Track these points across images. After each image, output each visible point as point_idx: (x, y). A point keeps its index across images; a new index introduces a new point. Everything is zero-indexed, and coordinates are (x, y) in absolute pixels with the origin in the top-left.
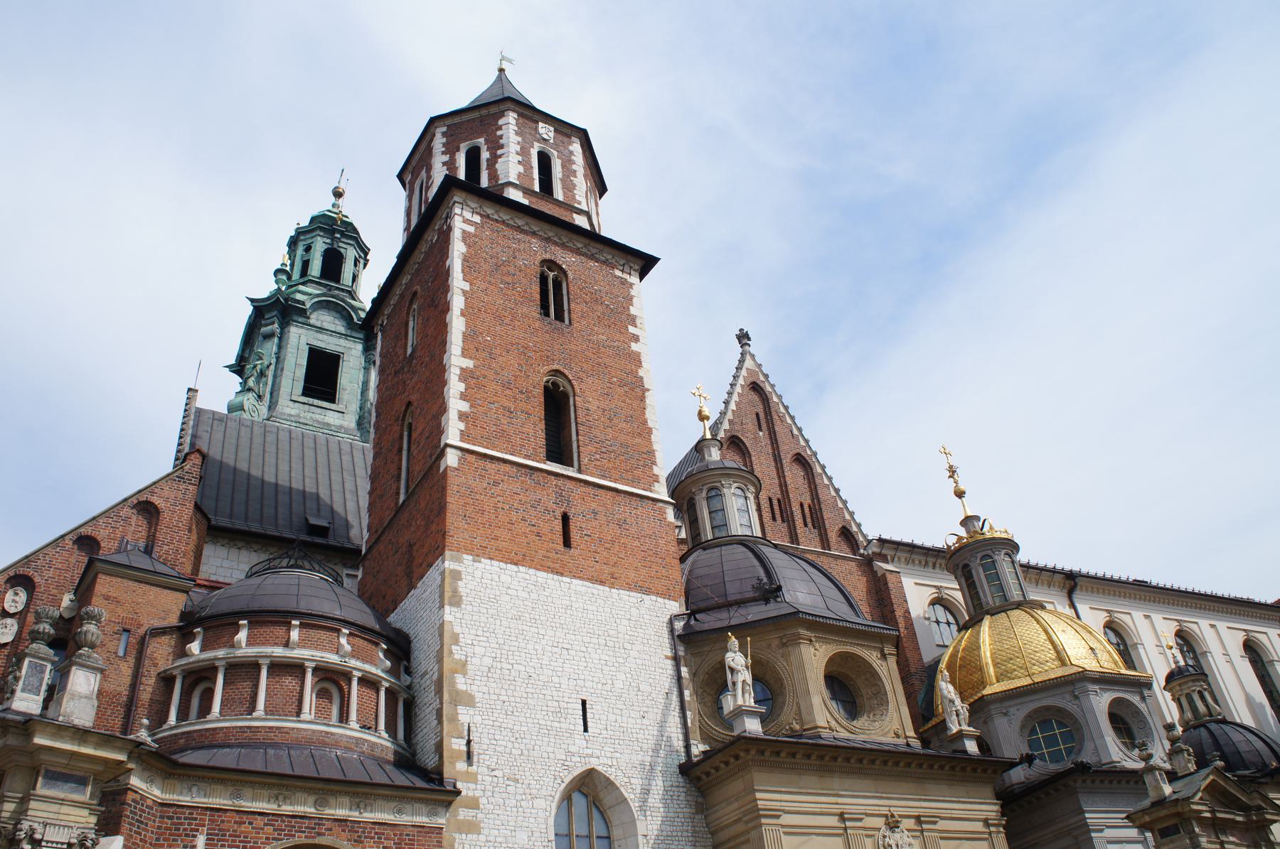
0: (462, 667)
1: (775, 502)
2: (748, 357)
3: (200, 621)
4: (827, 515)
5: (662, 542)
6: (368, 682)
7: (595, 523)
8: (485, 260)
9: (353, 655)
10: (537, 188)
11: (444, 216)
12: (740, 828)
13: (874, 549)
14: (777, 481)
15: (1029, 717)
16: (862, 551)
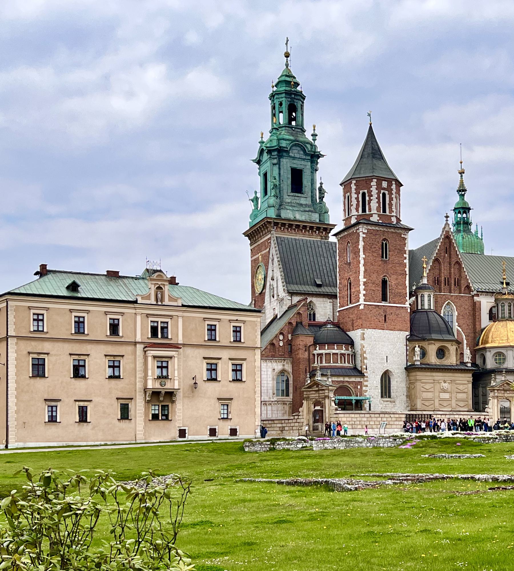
0: (365, 352)
1: (447, 279)
2: (447, 226)
3: (318, 344)
4: (462, 282)
5: (406, 317)
6: (348, 355)
7: (391, 316)
8: (368, 245)
9: (346, 350)
10: (382, 213)
11: (357, 228)
12: (414, 381)
13: (475, 292)
14: (449, 271)
15: (495, 353)
16: (472, 293)
